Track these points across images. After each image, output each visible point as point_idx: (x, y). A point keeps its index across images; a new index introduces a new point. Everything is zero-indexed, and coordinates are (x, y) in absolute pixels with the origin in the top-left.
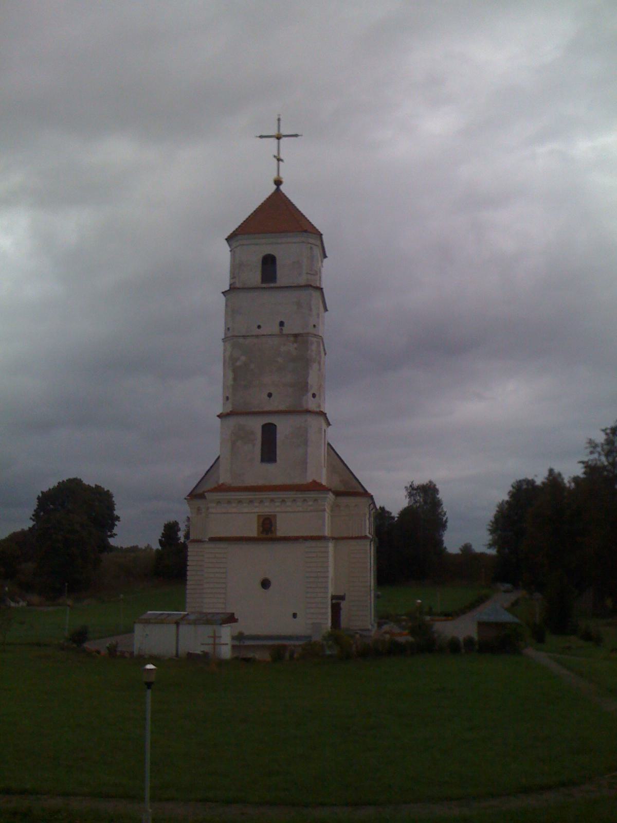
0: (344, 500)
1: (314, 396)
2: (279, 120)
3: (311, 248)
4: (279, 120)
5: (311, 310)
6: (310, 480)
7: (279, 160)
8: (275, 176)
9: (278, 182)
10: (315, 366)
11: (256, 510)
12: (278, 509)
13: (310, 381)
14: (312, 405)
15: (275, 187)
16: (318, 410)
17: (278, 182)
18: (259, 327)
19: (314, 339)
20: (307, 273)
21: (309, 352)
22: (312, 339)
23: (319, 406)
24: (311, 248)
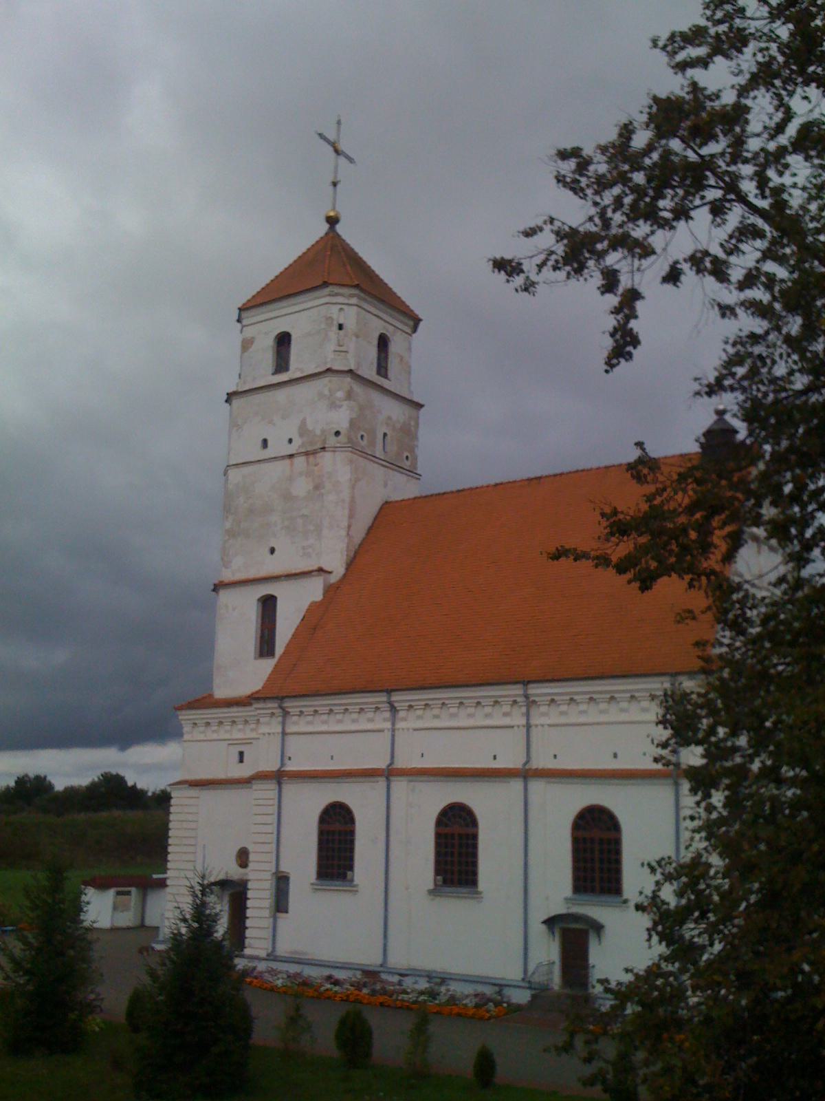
2: (339, 123)
4: (339, 123)
7: (335, 184)
9: (332, 221)
17: (332, 221)
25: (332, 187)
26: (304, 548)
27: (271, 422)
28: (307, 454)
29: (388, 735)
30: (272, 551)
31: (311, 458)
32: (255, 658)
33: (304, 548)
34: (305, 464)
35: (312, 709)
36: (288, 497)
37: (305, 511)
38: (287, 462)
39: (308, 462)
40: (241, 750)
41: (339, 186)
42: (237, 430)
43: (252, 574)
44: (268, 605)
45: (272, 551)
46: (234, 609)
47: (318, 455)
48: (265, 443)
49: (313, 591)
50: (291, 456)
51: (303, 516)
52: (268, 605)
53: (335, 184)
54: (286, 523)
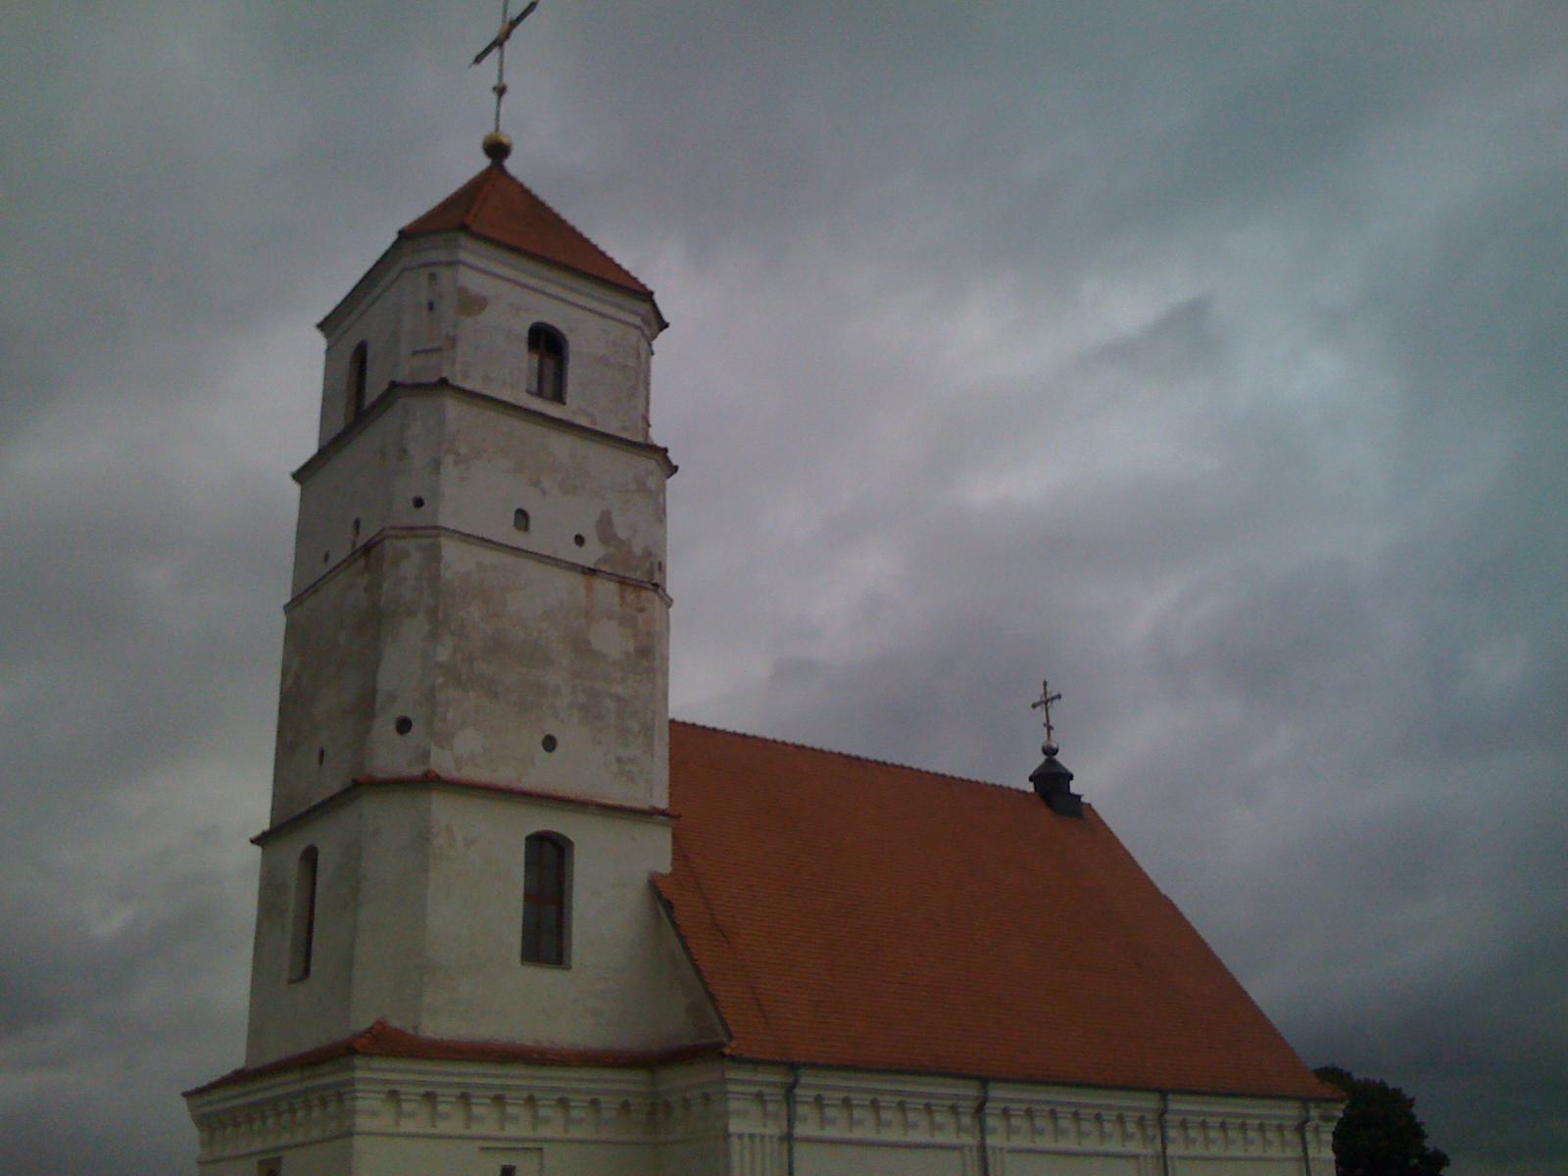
0: (678, 1080)
1: (404, 725)
3: (432, 277)
5: (403, 452)
6: (362, 1022)
7: (501, 91)
8: (486, 130)
9: (497, 150)
10: (413, 630)
11: (258, 1145)
12: (286, 1138)
13: (385, 682)
14: (390, 756)
15: (484, 162)
16: (417, 771)
17: (497, 150)
18: (327, 557)
19: (410, 544)
20: (415, 353)
21: (386, 585)
22: (401, 543)
23: (426, 755)
24: (432, 277)
25: (494, 97)
26: (619, 760)
27: (536, 484)
28: (623, 582)
29: (972, 1158)
30: (550, 743)
31: (630, 596)
32: (569, 968)
33: (619, 760)
34: (617, 599)
35: (841, 1095)
36: (581, 647)
37: (618, 689)
38: (577, 579)
39: (622, 597)
40: (507, 1163)
41: (506, 97)
42: (456, 463)
43: (504, 776)
44: (549, 858)
45: (550, 743)
46: (469, 843)
47: (643, 594)
48: (522, 518)
49: (653, 851)
50: (591, 572)
51: (615, 697)
52: (549, 858)
53: (501, 91)
54: (582, 699)
